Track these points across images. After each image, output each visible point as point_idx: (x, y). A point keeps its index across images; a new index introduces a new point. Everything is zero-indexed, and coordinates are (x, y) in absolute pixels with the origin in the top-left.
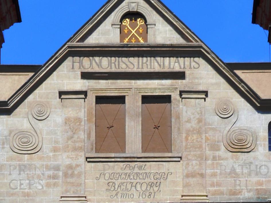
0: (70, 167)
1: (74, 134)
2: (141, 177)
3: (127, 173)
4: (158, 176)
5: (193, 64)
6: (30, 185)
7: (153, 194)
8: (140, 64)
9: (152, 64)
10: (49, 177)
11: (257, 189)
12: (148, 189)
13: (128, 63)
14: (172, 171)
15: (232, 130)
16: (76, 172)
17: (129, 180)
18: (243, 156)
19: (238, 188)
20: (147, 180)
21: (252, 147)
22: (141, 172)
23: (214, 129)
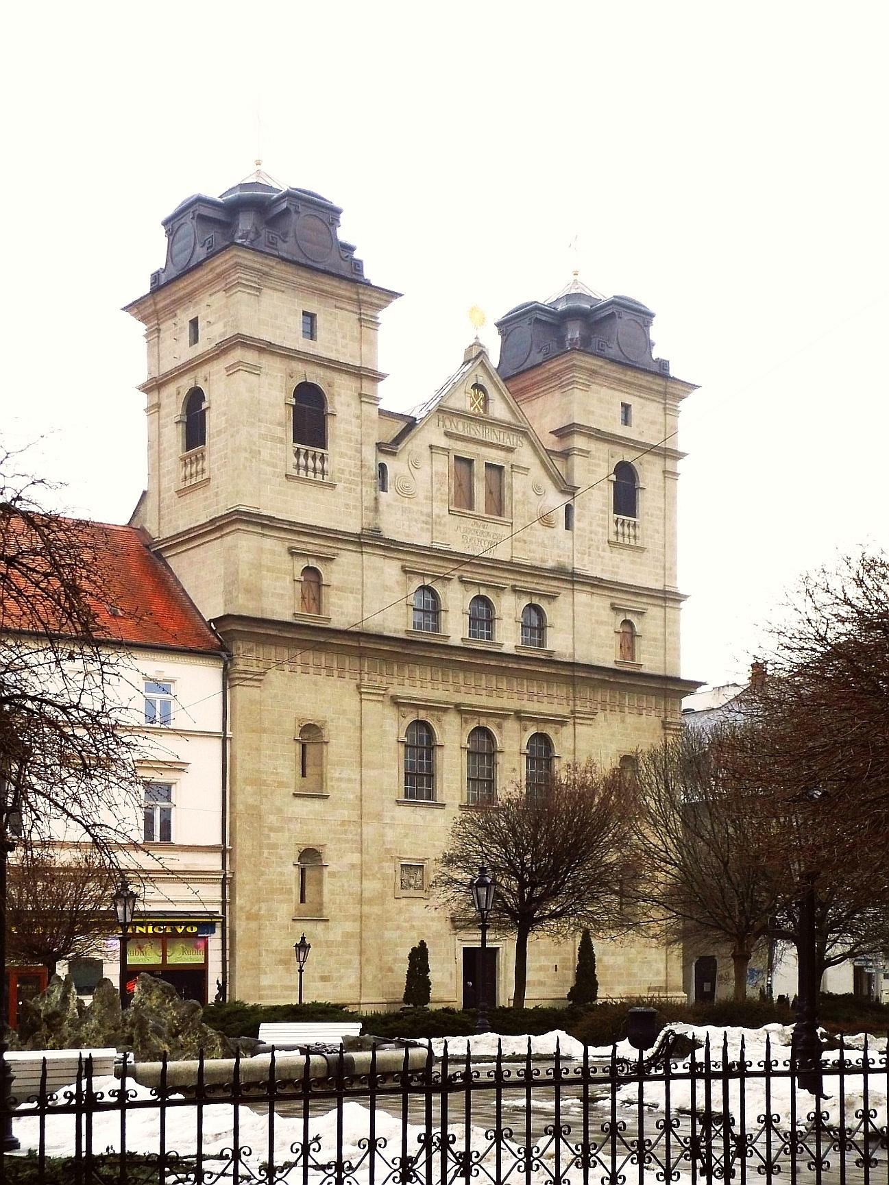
16: (443, 522)
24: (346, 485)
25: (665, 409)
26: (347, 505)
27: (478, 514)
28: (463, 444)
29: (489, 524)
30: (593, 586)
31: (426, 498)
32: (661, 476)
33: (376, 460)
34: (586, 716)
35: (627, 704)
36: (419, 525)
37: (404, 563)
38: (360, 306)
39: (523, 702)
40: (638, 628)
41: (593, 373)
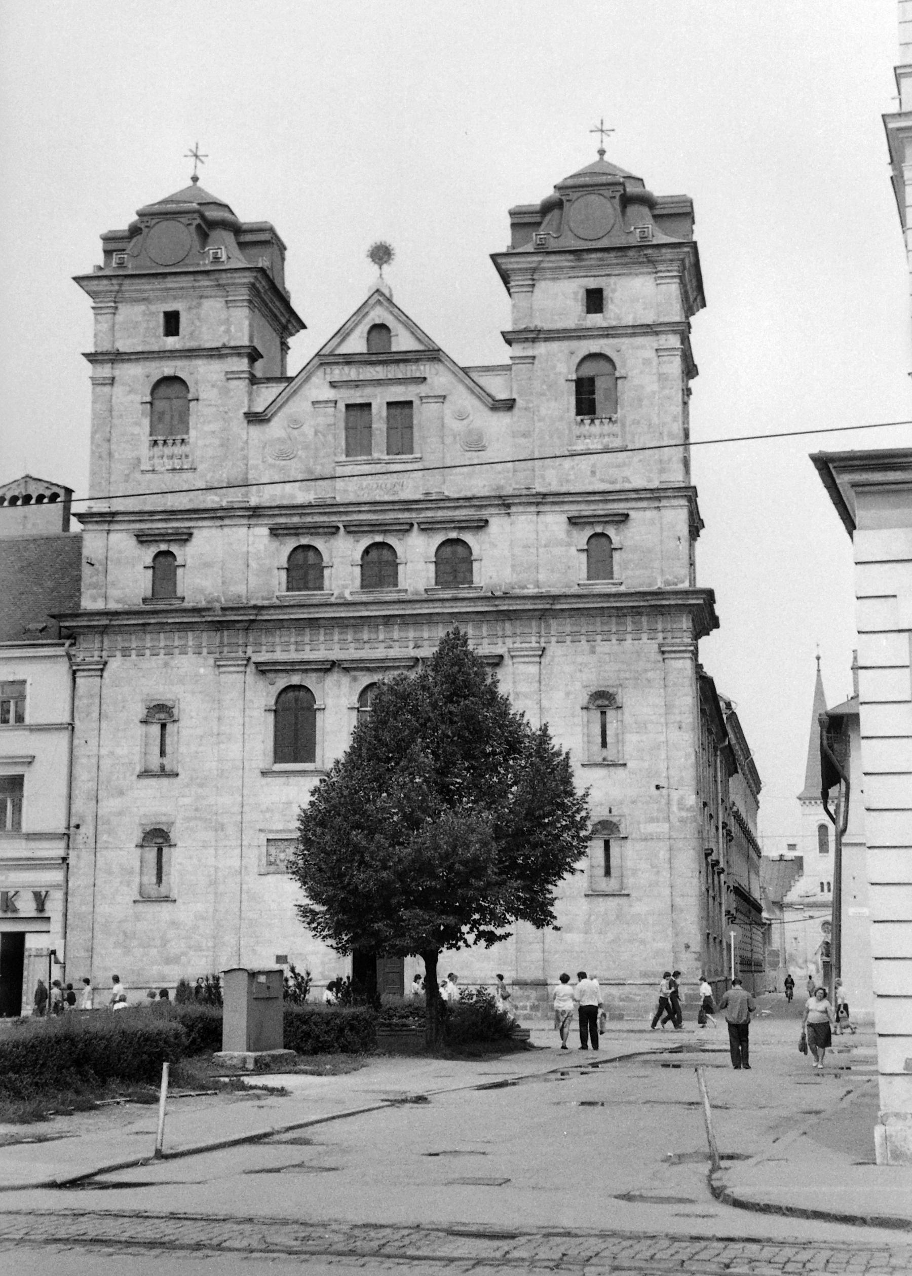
40: (616, 540)
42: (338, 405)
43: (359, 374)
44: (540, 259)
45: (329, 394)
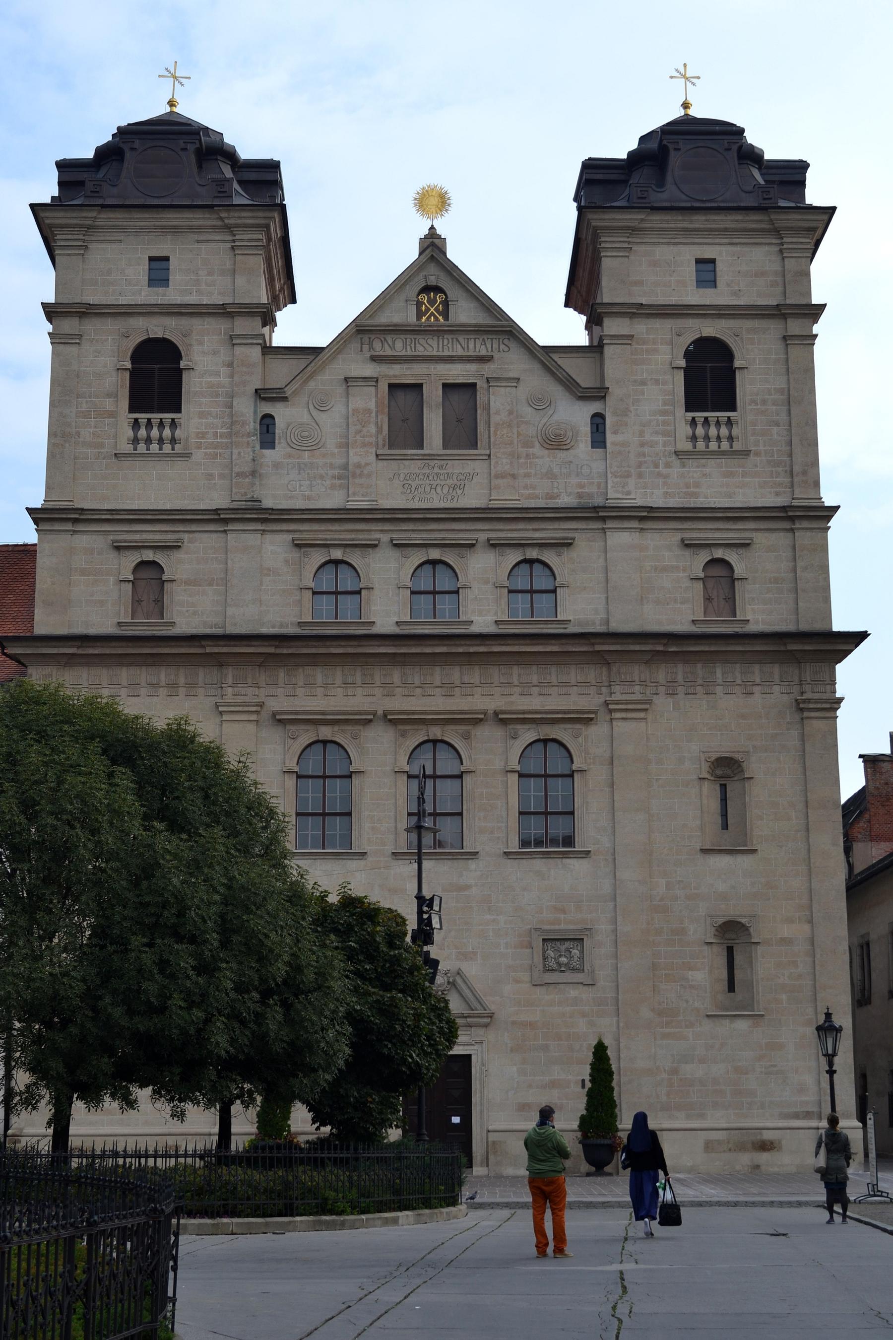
0: (358, 466)
1: (363, 427)
2: (442, 477)
3: (425, 474)
4: (462, 477)
5: (502, 347)
6: (311, 486)
7: (456, 498)
8: (441, 346)
9: (455, 346)
10: (334, 477)
11: (578, 493)
12: (451, 491)
13: (426, 346)
14: (479, 471)
15: (548, 424)
16: (365, 472)
17: (428, 482)
18: (561, 455)
19: (556, 491)
20: (449, 482)
21: (572, 444)
22: (442, 472)
23: (526, 423)
24: (208, 451)
25: (781, 251)
26: (211, 475)
27: (431, 452)
28: (405, 366)
29: (449, 462)
30: (642, 519)
31: (340, 446)
32: (779, 346)
33: (255, 412)
34: (630, 707)
35: (720, 681)
36: (328, 483)
37: (296, 536)
38: (232, 231)
39: (513, 698)
40: (739, 571)
41: (632, 231)
42: (380, 383)
43: (405, 347)
44: (643, 217)
45: (370, 370)
